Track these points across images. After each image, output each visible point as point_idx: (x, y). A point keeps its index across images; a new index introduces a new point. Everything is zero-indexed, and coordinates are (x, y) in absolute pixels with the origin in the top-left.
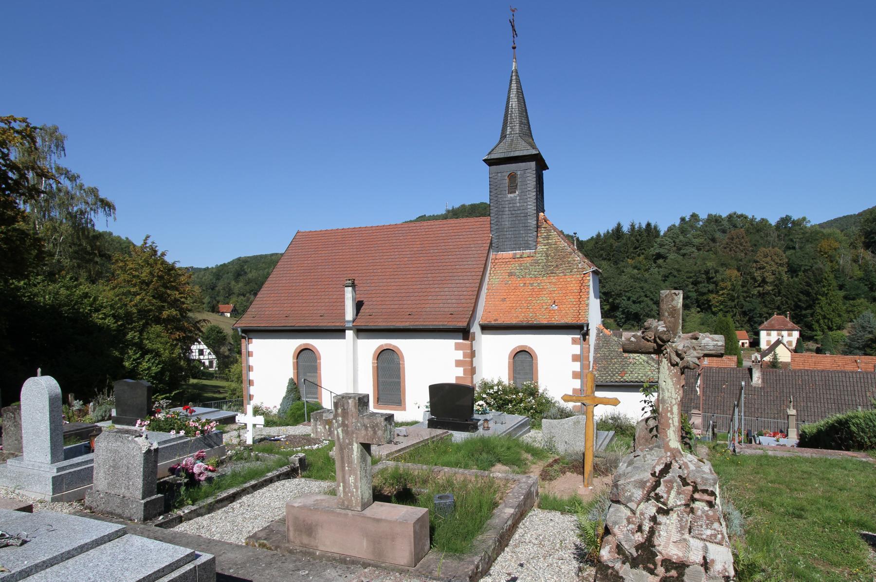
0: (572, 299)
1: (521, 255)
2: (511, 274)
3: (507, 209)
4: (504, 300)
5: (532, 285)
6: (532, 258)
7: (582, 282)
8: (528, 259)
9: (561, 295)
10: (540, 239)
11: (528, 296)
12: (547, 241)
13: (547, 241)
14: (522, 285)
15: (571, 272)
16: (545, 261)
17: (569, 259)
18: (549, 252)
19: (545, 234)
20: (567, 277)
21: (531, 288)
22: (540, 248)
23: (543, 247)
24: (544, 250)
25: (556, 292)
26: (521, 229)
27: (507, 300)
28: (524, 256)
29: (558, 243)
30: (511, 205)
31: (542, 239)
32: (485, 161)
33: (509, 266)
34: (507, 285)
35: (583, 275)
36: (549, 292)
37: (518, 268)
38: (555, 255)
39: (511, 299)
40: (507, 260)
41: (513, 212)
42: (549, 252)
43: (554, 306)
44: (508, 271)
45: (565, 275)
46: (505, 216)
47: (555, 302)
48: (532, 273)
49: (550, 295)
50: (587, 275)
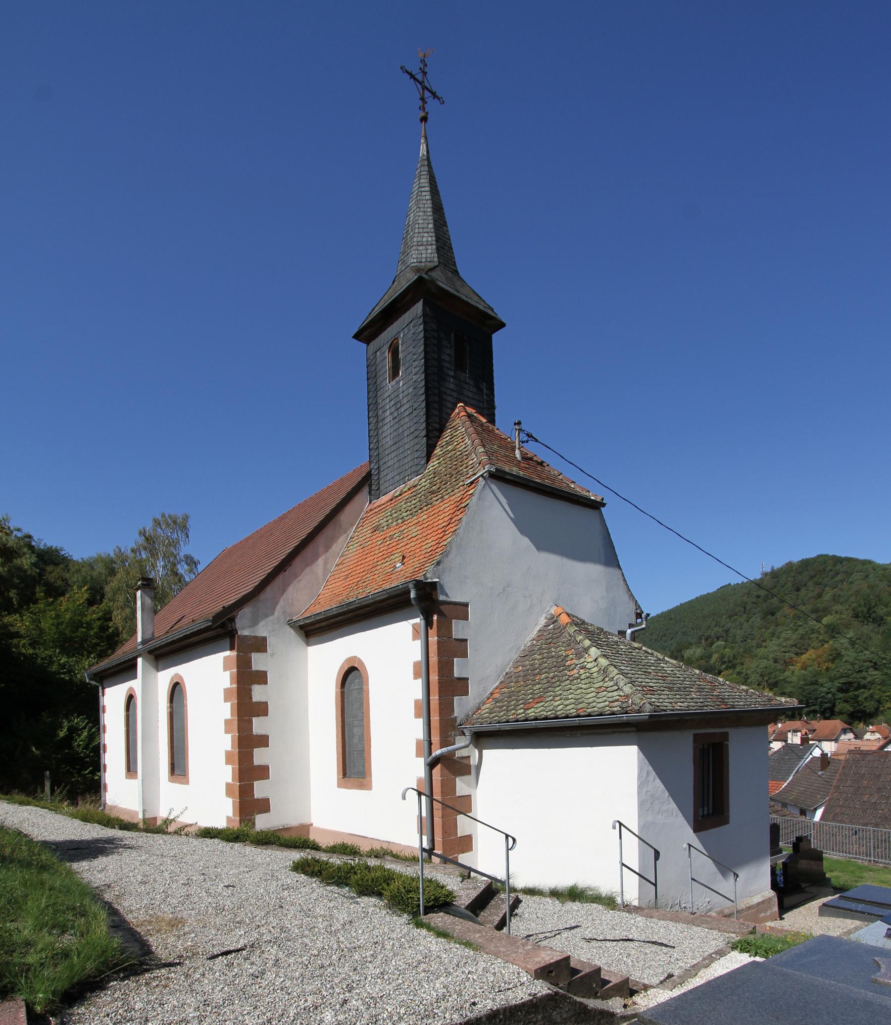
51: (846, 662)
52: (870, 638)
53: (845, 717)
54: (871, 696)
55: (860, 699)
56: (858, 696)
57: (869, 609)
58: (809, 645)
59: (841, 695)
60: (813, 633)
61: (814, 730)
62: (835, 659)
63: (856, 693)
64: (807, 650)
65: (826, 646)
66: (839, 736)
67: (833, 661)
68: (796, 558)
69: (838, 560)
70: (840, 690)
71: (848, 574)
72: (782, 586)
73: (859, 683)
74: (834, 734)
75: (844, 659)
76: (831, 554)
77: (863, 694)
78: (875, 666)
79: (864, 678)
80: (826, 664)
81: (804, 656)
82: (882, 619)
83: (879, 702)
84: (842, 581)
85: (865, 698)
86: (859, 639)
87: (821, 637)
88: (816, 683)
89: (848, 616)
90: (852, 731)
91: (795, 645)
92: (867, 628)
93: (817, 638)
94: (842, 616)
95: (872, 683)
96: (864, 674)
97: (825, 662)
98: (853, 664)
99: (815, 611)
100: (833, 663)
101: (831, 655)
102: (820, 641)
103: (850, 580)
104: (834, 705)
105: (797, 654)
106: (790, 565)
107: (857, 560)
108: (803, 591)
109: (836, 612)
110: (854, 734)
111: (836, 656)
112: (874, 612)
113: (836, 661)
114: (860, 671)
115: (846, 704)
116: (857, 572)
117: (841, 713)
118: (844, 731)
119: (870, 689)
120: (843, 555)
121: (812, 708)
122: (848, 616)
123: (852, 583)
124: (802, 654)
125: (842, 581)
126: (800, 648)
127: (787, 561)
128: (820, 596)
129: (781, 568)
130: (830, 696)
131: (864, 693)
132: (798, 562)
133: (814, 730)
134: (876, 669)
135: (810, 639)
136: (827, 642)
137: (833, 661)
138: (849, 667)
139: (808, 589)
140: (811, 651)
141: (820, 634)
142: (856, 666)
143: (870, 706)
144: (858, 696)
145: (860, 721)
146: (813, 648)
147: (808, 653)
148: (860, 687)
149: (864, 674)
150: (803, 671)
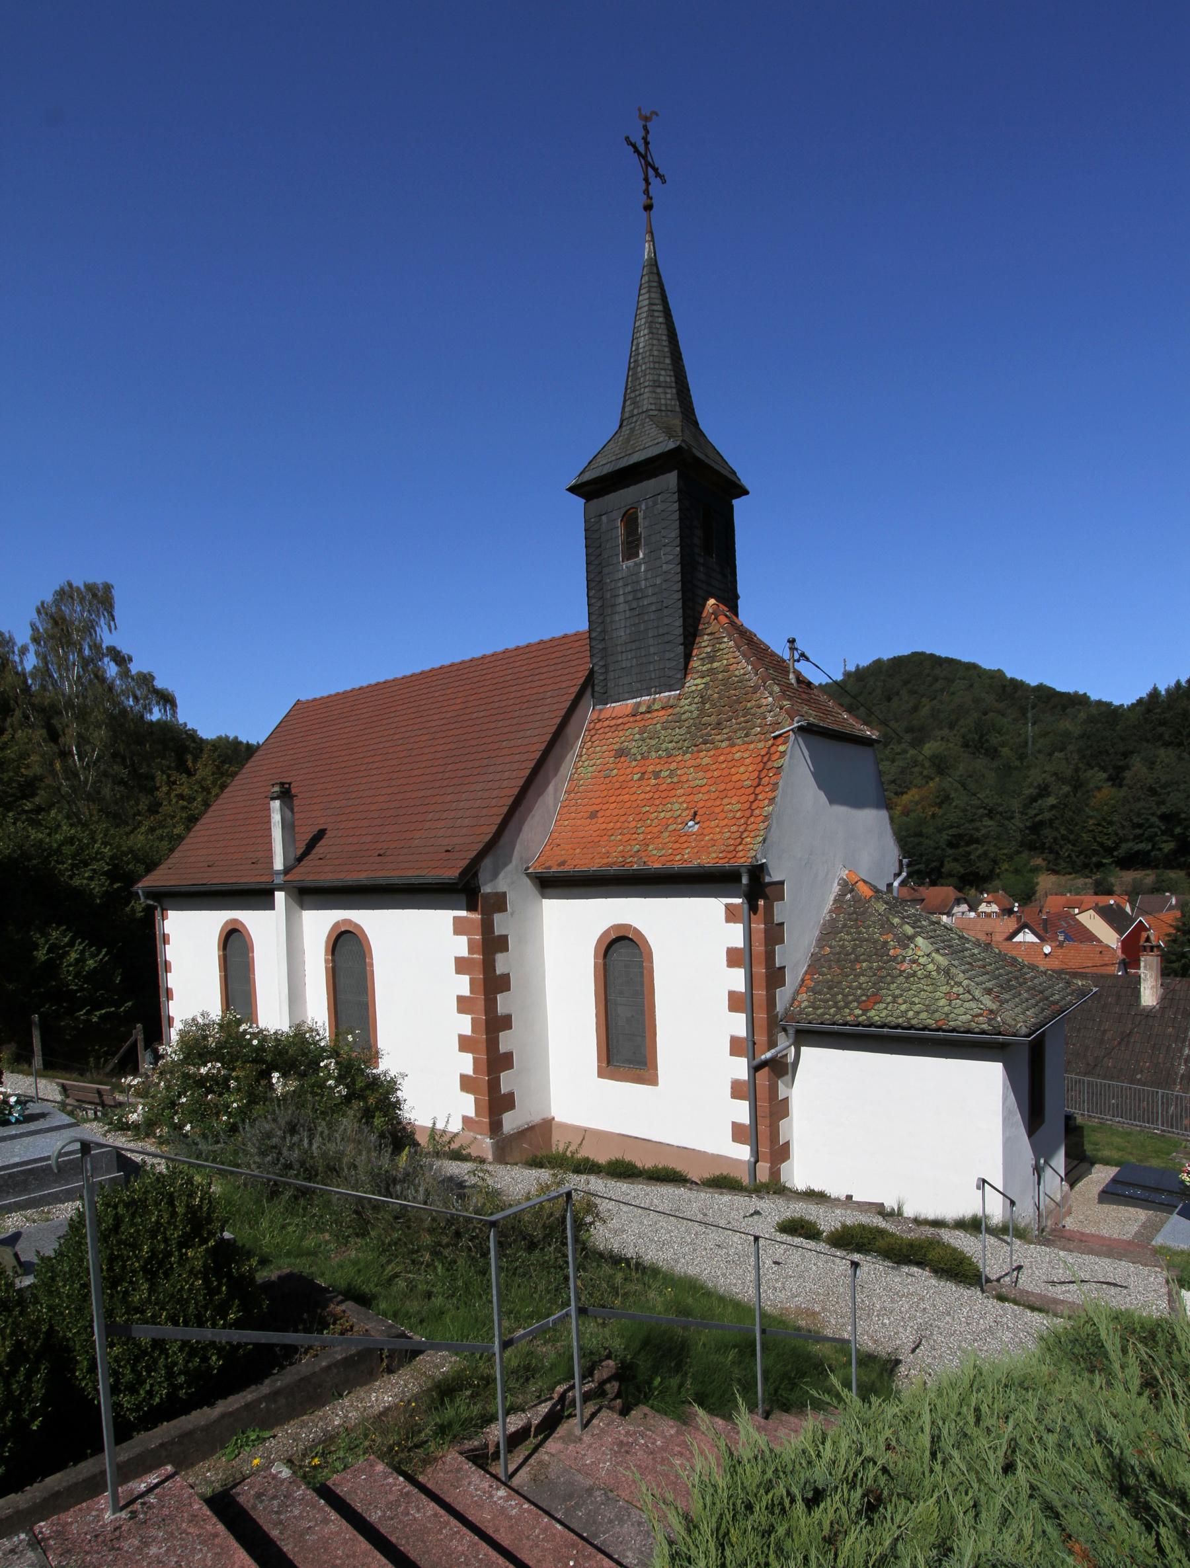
0: (734, 804)
1: (649, 707)
2: (621, 753)
3: (621, 599)
4: (593, 815)
5: (656, 775)
6: (670, 711)
7: (765, 759)
8: (663, 713)
9: (713, 796)
10: (695, 663)
11: (644, 802)
12: (709, 666)
13: (709, 666)
14: (636, 777)
15: (747, 735)
16: (696, 713)
17: (749, 705)
18: (709, 692)
19: (709, 649)
20: (734, 750)
21: (653, 782)
22: (694, 683)
23: (698, 681)
24: (699, 687)
25: (704, 790)
26: (651, 641)
27: (600, 814)
28: (656, 707)
29: (731, 668)
30: (629, 589)
31: (699, 663)
32: (572, 490)
33: (621, 734)
34: (607, 781)
35: (770, 742)
36: (690, 790)
37: (637, 736)
38: (720, 698)
39: (608, 813)
40: (620, 721)
41: (634, 605)
42: (709, 692)
43: (691, 823)
44: (616, 747)
45: (733, 745)
46: (617, 617)
47: (695, 814)
48: (664, 746)
49: (689, 798)
50: (781, 740)
51: (956, 807)
52: (983, 776)
53: (954, 880)
54: (985, 854)
55: (972, 857)
56: (969, 853)
57: (982, 736)
59: (950, 851)
60: (916, 766)
61: (923, 900)
62: (942, 802)
63: (968, 849)
65: (931, 784)
66: (952, 908)
67: (940, 805)
68: (887, 655)
69: (936, 661)
70: (950, 844)
71: (949, 681)
72: (870, 693)
73: (972, 836)
75: (954, 804)
77: (976, 851)
78: (991, 814)
79: (978, 830)
80: (933, 809)
81: (905, 797)
82: (996, 751)
83: (995, 862)
84: (942, 690)
85: (979, 857)
86: (970, 776)
87: (925, 773)
88: (920, 834)
89: (956, 745)
90: (966, 902)
91: (894, 782)
92: (981, 763)
93: (921, 773)
94: (951, 745)
95: (986, 836)
96: (978, 824)
98: (964, 811)
99: (909, 730)
100: (940, 807)
101: (938, 797)
102: (925, 777)
103: (952, 689)
104: (942, 865)
105: (896, 794)
106: (878, 663)
109: (942, 739)
110: (969, 906)
111: (944, 799)
112: (987, 741)
113: (944, 806)
114: (972, 821)
115: (955, 864)
116: (960, 679)
117: (950, 875)
118: (958, 902)
119: (983, 845)
120: (943, 655)
121: (917, 867)
122: (956, 745)
124: (902, 793)
125: (942, 690)
126: (900, 786)
128: (915, 709)
129: (868, 667)
130: (939, 852)
131: (976, 849)
132: (889, 660)
133: (923, 900)
134: (991, 818)
135: (911, 774)
136: (932, 779)
139: (900, 700)
140: (914, 791)
141: (923, 766)
143: (983, 867)
144: (969, 853)
145: (972, 886)
146: (916, 786)
148: (973, 841)
149: (978, 824)
150: (905, 818)
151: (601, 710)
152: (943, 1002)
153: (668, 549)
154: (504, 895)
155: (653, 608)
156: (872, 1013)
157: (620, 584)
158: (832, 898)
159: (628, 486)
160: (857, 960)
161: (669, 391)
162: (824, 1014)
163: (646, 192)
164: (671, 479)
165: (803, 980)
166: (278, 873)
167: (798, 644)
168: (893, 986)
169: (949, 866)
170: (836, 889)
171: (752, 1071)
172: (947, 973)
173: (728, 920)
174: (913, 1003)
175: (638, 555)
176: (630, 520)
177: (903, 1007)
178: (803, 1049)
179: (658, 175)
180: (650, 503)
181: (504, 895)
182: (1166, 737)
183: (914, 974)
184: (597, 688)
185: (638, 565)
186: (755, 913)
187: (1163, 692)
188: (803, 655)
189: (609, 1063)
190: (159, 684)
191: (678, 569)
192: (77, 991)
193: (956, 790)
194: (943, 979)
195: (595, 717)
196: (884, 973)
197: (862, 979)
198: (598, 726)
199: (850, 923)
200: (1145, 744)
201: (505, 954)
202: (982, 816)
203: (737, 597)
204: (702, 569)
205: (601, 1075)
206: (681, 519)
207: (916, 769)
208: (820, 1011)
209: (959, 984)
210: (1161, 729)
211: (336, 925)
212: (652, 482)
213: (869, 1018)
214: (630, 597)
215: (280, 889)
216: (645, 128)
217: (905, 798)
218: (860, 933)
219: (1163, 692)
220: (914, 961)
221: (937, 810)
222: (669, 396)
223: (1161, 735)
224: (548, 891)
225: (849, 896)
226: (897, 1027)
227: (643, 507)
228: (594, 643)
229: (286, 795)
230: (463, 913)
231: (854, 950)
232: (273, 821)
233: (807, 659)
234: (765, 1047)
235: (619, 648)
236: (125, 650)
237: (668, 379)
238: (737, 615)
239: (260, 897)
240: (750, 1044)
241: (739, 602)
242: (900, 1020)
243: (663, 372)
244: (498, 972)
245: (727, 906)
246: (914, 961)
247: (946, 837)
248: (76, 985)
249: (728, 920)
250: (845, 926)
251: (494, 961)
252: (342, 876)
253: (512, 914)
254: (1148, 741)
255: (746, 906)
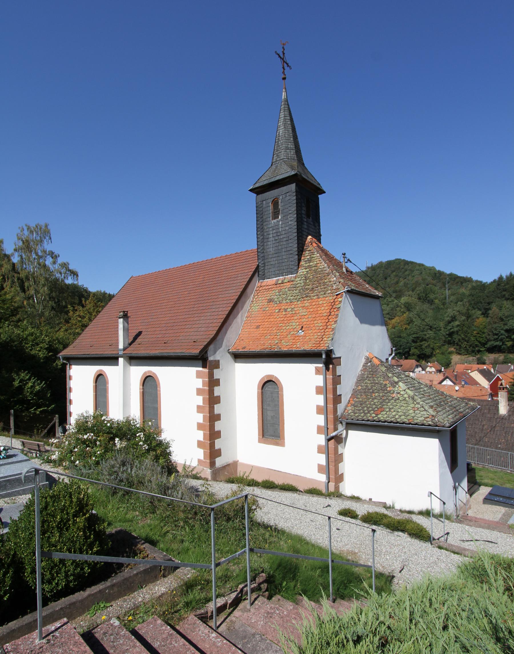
0: (319, 323)
1: (283, 281)
2: (270, 301)
3: (271, 236)
4: (258, 327)
5: (286, 310)
6: (292, 283)
7: (333, 304)
8: (289, 283)
9: (310, 320)
10: (302, 263)
11: (280, 322)
12: (308, 264)
13: (308, 264)
14: (277, 311)
15: (325, 294)
16: (303, 284)
17: (326, 281)
18: (309, 275)
19: (308, 257)
20: (319, 300)
21: (284, 313)
22: (302, 271)
23: (304, 270)
24: (304, 273)
25: (306, 317)
26: (284, 253)
27: (261, 327)
28: (286, 281)
29: (318, 265)
30: (275, 231)
31: (304, 263)
33: (270, 292)
34: (264, 312)
35: (335, 297)
36: (299, 317)
37: (277, 294)
38: (313, 278)
39: (264, 326)
40: (270, 287)
41: (277, 238)
42: (309, 275)
43: (300, 331)
44: (268, 298)
45: (318, 298)
46: (269, 243)
47: (302, 327)
48: (289, 298)
49: (300, 321)
50: (339, 296)
51: (416, 325)
52: (427, 312)
53: (415, 357)
54: (429, 345)
56: (422, 345)
57: (426, 295)
58: (396, 314)
59: (413, 344)
61: (402, 366)
63: (421, 343)
64: (395, 317)
65: (405, 315)
66: (414, 369)
67: (408, 324)
68: (385, 260)
69: (406, 263)
70: (414, 341)
71: (412, 271)
73: (423, 338)
74: (412, 368)
76: (402, 259)
77: (425, 344)
78: (431, 328)
79: (425, 335)
81: (393, 320)
82: (432, 301)
83: (433, 349)
84: (409, 275)
85: (426, 347)
86: (422, 312)
87: (402, 310)
88: (400, 337)
90: (421, 366)
91: (388, 314)
92: (426, 306)
93: (400, 310)
95: (429, 338)
96: (425, 333)
97: (404, 324)
98: (419, 327)
99: (395, 292)
100: (409, 325)
103: (413, 275)
104: (410, 350)
105: (389, 319)
106: (381, 263)
107: (416, 263)
108: (388, 280)
109: (409, 296)
110: (422, 368)
111: (410, 322)
112: (429, 297)
114: (423, 331)
115: (416, 350)
117: (413, 355)
118: (417, 366)
119: (428, 342)
120: (409, 260)
121: (399, 351)
123: (413, 276)
124: (392, 319)
125: (409, 275)
126: (391, 316)
127: (380, 261)
128: (397, 283)
129: (377, 265)
130: (408, 344)
131: (425, 343)
133: (402, 366)
134: (431, 330)
136: (405, 313)
137: (408, 324)
138: (418, 328)
140: (397, 318)
141: (401, 307)
142: (422, 328)
143: (428, 351)
144: (422, 345)
146: (398, 316)
147: (395, 319)
148: (423, 340)
149: (425, 333)
151: (262, 282)
152: (411, 411)
153: (291, 215)
154: (219, 361)
155: (285, 239)
156: (380, 416)
157: (271, 229)
158: (362, 364)
159: (275, 189)
160: (373, 392)
161: (292, 151)
162: (358, 416)
163: (284, 73)
164: (293, 187)
165: (349, 401)
166: (121, 350)
167: (346, 255)
168: (389, 404)
169: (413, 351)
170: (363, 361)
171: (327, 441)
172: (413, 398)
173: (316, 374)
174: (398, 412)
175: (278, 218)
176: (275, 203)
177: (394, 413)
178: (349, 431)
179: (288, 66)
180: (284, 196)
181: (219, 361)
182: (507, 296)
183: (398, 399)
184: (260, 273)
185: (278, 222)
186: (328, 371)
187: (505, 277)
188: (349, 260)
189: (263, 436)
190: (71, 267)
191: (296, 223)
192: (31, 400)
193: (415, 318)
194: (411, 401)
195: (259, 285)
196: (385, 398)
197: (375, 401)
198: (261, 289)
199: (370, 376)
200: (497, 299)
201: (218, 387)
202: (428, 329)
203: (320, 235)
204: (305, 223)
205: (260, 441)
206: (297, 203)
207: (398, 309)
208: (357, 415)
209: (418, 403)
210: (504, 293)
211: (145, 373)
212: (285, 188)
213: (378, 418)
214: (275, 235)
215: (121, 357)
216: (283, 48)
217: (393, 321)
218: (374, 380)
219: (505, 277)
220: (398, 393)
221: (407, 326)
222: (292, 153)
223: (504, 295)
224: (238, 360)
225: (369, 364)
226: (391, 422)
227: (281, 198)
228: (259, 254)
229: (125, 316)
230: (201, 369)
231: (372, 387)
232: (119, 327)
233: (351, 262)
234: (333, 430)
235: (270, 256)
236: (56, 253)
237: (292, 146)
238: (320, 243)
239: (112, 360)
240: (326, 429)
241: (321, 237)
242: (392, 419)
243: (290, 144)
244: (215, 395)
245: (316, 368)
246: (398, 393)
247: (411, 338)
248: (31, 397)
249: (316, 374)
250: (367, 377)
251: (213, 390)
252: (148, 352)
253: (222, 370)
254: (499, 298)
255: (324, 368)
